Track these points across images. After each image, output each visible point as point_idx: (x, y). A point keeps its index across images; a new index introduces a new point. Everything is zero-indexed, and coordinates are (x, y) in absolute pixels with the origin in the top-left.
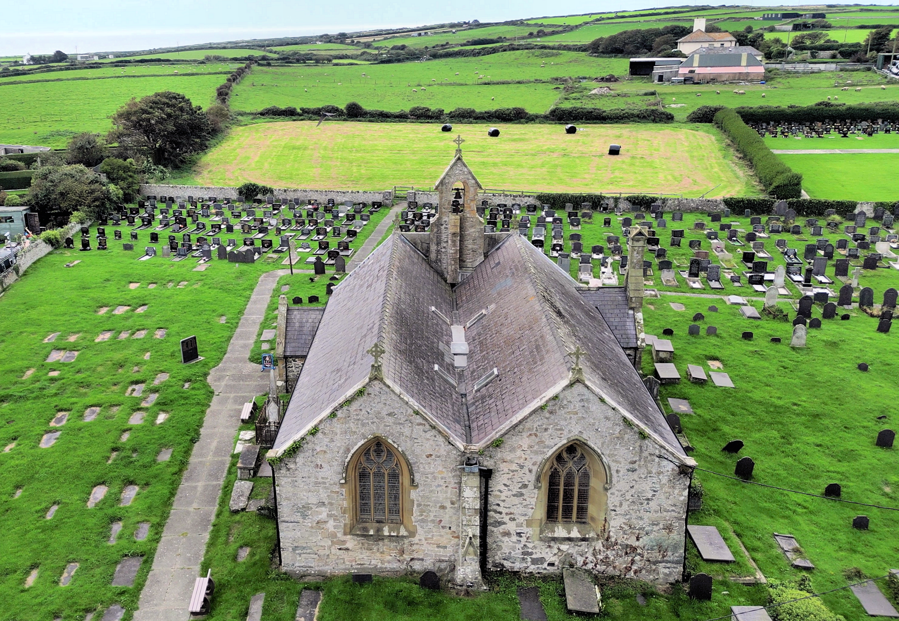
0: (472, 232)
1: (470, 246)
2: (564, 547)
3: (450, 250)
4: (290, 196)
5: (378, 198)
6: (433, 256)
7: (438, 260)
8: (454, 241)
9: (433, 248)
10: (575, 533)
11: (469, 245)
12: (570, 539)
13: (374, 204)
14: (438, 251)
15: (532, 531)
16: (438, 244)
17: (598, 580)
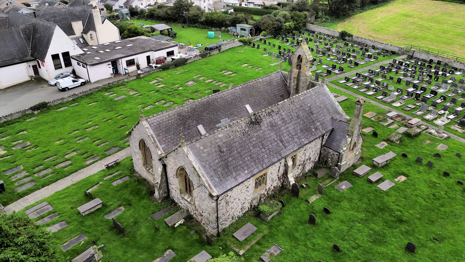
0: (302, 78)
1: (301, 85)
2: (186, 202)
3: (293, 84)
4: (359, 40)
5: (396, 50)
6: (288, 84)
7: (289, 87)
8: (294, 81)
9: (288, 81)
10: (189, 200)
11: (301, 84)
12: (186, 200)
13: (392, 52)
14: (290, 83)
15: (178, 192)
16: (290, 80)
17: (189, 218)
